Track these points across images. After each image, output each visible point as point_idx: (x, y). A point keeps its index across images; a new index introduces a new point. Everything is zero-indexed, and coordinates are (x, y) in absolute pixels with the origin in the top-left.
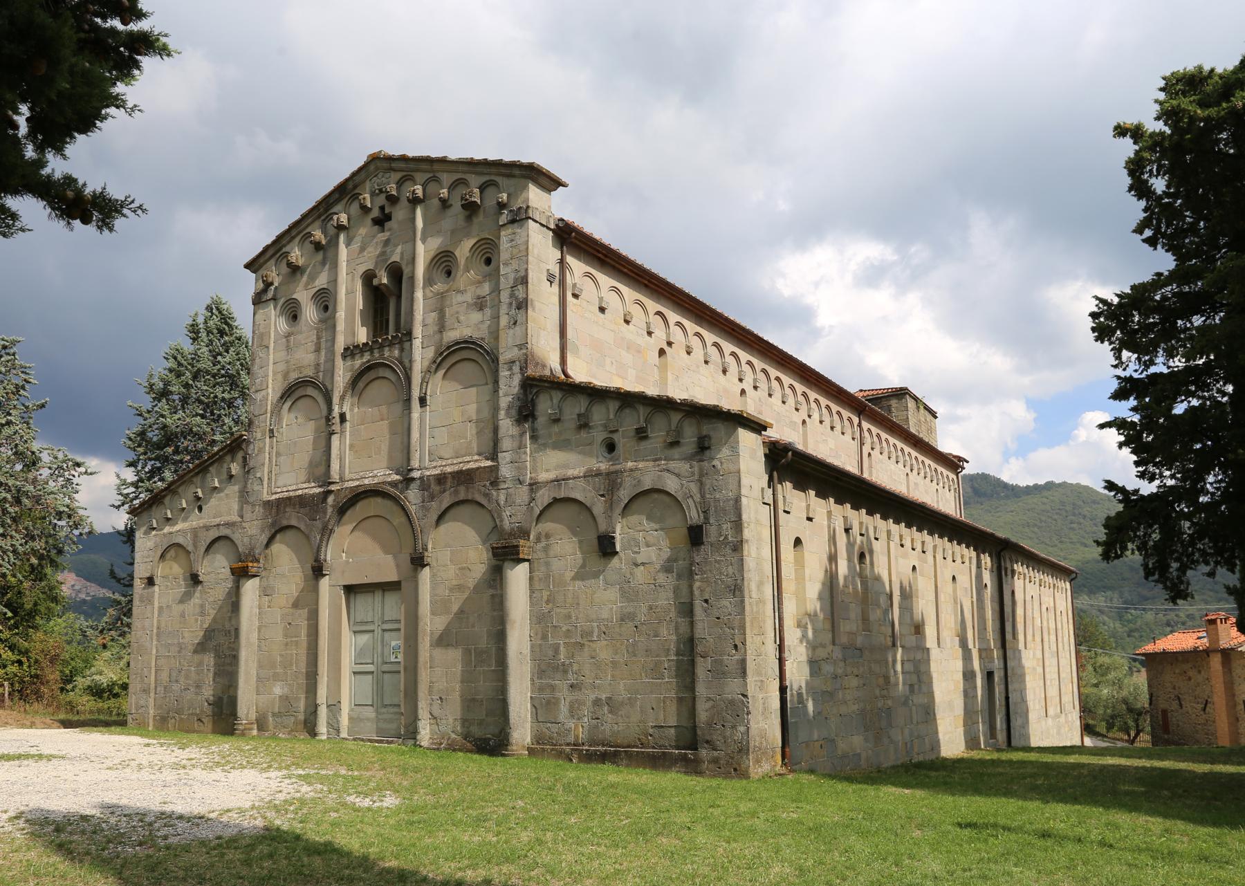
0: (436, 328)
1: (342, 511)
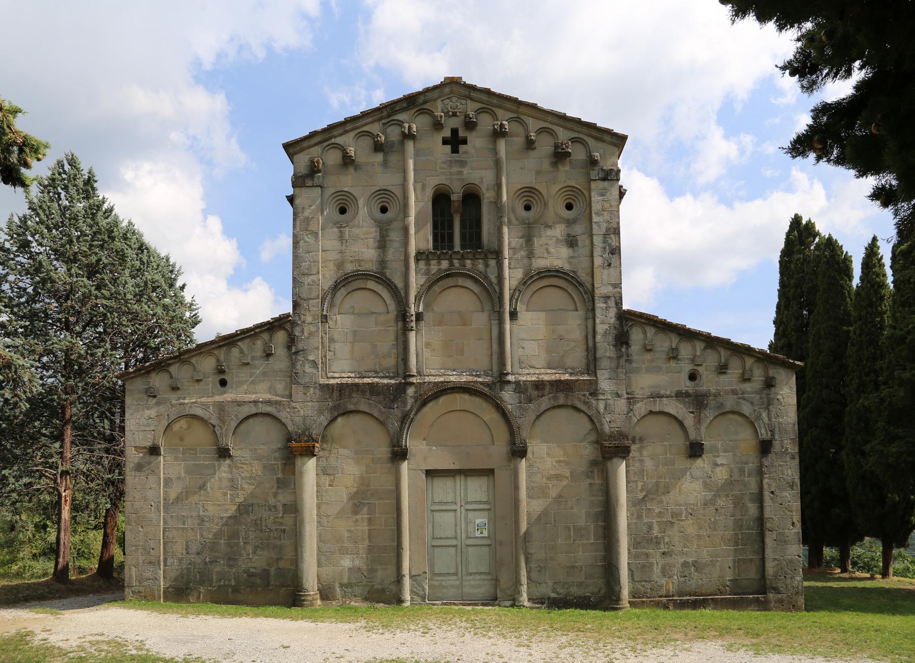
1: (423, 402)
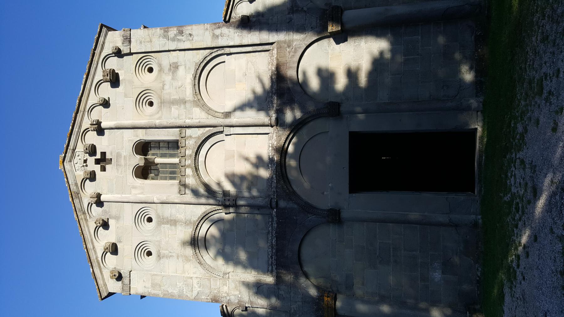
0: (182, 106)
1: (292, 195)
